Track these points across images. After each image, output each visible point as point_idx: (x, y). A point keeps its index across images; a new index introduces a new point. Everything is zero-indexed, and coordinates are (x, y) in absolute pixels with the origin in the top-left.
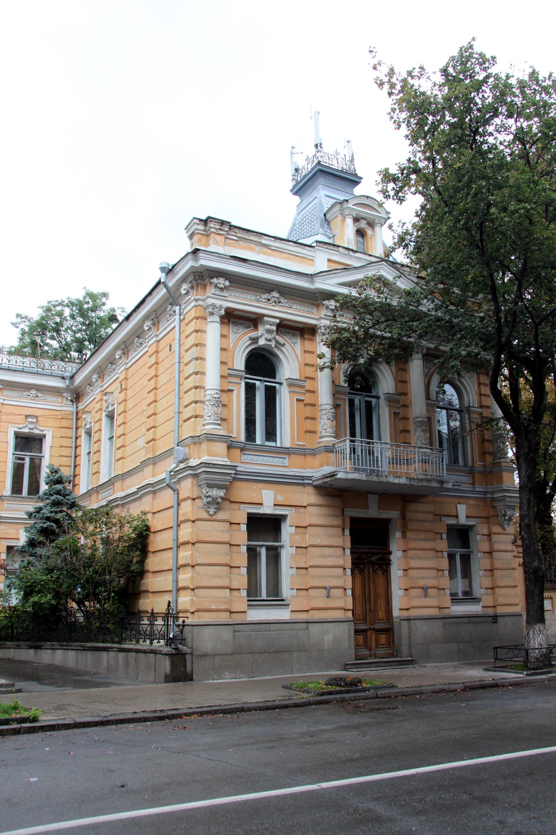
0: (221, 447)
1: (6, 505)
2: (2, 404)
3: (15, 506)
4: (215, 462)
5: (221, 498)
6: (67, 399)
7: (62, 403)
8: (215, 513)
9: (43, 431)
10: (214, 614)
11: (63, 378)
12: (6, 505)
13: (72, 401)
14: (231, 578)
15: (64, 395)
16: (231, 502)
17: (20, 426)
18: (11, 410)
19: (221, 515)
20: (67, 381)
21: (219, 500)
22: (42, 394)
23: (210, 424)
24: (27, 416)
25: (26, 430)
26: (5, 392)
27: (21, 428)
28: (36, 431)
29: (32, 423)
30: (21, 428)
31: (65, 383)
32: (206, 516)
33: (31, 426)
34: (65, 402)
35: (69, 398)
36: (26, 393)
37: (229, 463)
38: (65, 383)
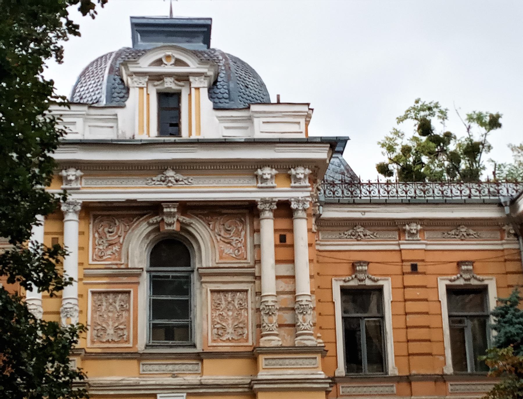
1: (450, 387)
2: (425, 250)
3: (462, 387)
6: (509, 233)
7: (502, 239)
9: (483, 280)
11: (500, 205)
12: (450, 387)
13: (516, 235)
15: (504, 228)
17: (453, 277)
20: (507, 210)
22: (474, 230)
24: (459, 264)
25: (461, 282)
26: (426, 235)
27: (454, 280)
28: (474, 282)
29: (467, 271)
30: (454, 280)
31: (503, 211)
33: (467, 276)
34: (506, 238)
35: (512, 232)
36: (453, 232)
38: (503, 211)
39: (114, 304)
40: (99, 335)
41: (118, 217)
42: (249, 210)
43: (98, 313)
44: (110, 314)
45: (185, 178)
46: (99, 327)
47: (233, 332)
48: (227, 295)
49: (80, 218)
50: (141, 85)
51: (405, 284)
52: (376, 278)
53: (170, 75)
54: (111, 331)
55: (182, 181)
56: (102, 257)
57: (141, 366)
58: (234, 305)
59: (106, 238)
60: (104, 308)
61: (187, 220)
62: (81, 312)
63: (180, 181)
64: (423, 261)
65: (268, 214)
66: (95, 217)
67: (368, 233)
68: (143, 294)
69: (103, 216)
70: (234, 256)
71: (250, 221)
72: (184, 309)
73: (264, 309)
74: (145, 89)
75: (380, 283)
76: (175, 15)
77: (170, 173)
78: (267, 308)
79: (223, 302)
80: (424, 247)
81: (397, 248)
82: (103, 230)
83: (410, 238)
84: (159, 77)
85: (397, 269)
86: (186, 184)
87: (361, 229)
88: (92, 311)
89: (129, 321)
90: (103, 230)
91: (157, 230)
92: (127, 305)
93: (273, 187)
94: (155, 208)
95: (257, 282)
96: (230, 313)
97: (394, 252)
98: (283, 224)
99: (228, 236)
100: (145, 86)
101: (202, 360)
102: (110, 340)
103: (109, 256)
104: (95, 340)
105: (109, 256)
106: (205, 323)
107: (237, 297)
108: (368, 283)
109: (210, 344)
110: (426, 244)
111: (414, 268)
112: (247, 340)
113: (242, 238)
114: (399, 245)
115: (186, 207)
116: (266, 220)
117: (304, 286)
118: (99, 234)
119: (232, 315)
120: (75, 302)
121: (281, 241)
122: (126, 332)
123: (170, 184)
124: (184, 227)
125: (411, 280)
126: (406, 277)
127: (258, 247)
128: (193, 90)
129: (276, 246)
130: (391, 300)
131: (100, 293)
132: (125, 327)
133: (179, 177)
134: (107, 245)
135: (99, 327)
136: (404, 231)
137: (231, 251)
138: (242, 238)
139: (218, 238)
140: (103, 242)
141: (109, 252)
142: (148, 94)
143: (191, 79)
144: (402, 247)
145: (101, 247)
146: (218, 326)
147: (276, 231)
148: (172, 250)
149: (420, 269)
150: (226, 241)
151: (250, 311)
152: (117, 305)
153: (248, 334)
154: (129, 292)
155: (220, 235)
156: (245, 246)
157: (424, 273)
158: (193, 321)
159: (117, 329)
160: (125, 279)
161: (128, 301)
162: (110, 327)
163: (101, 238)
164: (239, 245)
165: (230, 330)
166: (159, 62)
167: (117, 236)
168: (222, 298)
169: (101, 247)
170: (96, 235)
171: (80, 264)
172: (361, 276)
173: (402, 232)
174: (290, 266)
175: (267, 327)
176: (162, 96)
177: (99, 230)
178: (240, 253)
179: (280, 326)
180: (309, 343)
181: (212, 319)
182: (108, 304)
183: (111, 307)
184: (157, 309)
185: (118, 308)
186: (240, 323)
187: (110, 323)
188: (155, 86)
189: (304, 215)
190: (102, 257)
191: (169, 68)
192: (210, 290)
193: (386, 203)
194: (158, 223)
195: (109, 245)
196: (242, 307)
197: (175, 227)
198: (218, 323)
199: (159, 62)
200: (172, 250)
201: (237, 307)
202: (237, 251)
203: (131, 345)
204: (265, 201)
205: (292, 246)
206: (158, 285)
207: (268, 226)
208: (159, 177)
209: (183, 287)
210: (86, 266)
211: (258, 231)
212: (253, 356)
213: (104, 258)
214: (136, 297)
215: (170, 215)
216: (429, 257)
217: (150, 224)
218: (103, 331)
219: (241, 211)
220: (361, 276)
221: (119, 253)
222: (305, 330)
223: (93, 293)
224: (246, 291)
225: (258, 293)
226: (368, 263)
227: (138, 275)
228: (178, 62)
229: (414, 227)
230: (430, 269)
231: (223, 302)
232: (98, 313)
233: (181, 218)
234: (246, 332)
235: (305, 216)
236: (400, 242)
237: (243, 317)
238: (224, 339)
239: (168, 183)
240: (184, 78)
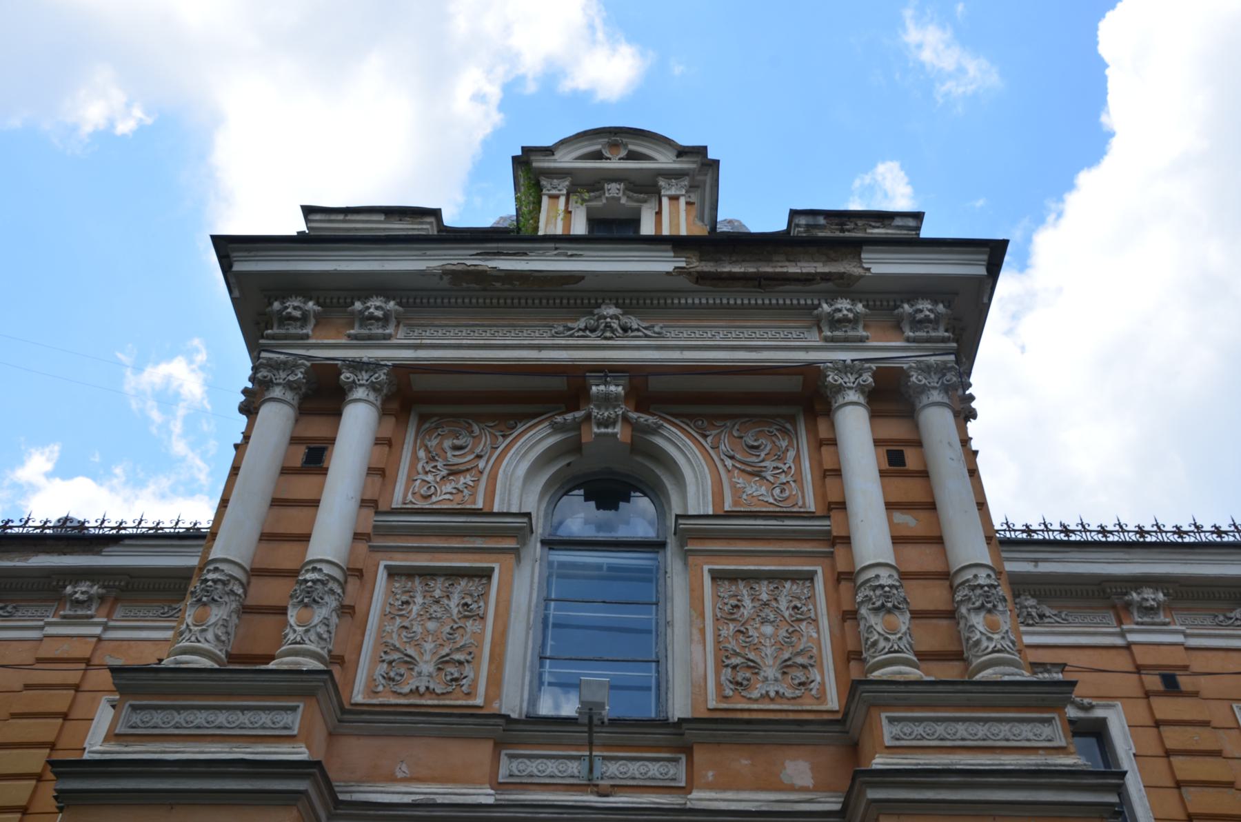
2: (1188, 649)
18: (1215, 663)
39: (445, 601)
40: (392, 674)
41: (479, 418)
43: (398, 620)
44: (431, 625)
45: (645, 324)
46: (396, 656)
47: (779, 676)
48: (756, 587)
49: (384, 412)
50: (554, 192)
51: (1159, 716)
52: (1086, 701)
54: (427, 667)
55: (638, 330)
56: (430, 496)
57: (504, 760)
58: (777, 610)
59: (446, 459)
60: (415, 609)
62: (346, 610)
63: (633, 331)
64: (1185, 668)
65: (852, 396)
66: (423, 419)
69: (442, 416)
70: (771, 500)
71: (808, 431)
73: (868, 599)
74: (562, 200)
75: (1099, 713)
78: (878, 592)
79: (747, 602)
80: (1179, 639)
81: (1118, 641)
82: (440, 443)
83: (1146, 619)
86: (646, 336)
88: (384, 615)
89: (480, 646)
90: (440, 443)
91: (574, 447)
92: (482, 604)
93: (862, 339)
95: (840, 551)
96: (768, 629)
97: (1113, 652)
98: (895, 430)
99: (754, 459)
100: (565, 192)
101: (688, 750)
102: (422, 689)
103: (447, 496)
104: (380, 688)
105: (447, 496)
106: (697, 649)
107: (785, 592)
109: (712, 704)
110: (1186, 635)
112: (821, 697)
113: (790, 462)
114: (1122, 634)
116: (849, 409)
118: (427, 450)
119: (775, 635)
120: (337, 573)
121: (891, 464)
122: (468, 670)
123: (608, 334)
124: (642, 447)
125: (1167, 708)
126: (1155, 701)
127: (833, 473)
128: (665, 201)
129: (883, 474)
130: (1134, 751)
131: (411, 573)
132: (469, 658)
133: (634, 322)
134: (445, 472)
135: (396, 656)
136: (1128, 606)
137: (763, 490)
138: (790, 462)
139: (729, 462)
140: (435, 467)
141: (448, 487)
143: (662, 182)
144: (1132, 638)
145: (430, 478)
146: (735, 661)
147: (877, 443)
149: (1184, 682)
150: (749, 469)
151: (824, 623)
152: (454, 604)
153: (822, 684)
154: (486, 574)
155: (732, 458)
156: (798, 480)
157: (1195, 694)
158: (662, 661)
159: (443, 662)
160: (479, 543)
161: (484, 596)
162: (427, 657)
163: (433, 459)
164: (783, 478)
165: (771, 672)
167: (472, 456)
168: (745, 592)
169: (430, 478)
170: (422, 454)
173: (1121, 611)
174: (923, 515)
175: (882, 644)
177: (429, 444)
178: (787, 493)
181: (718, 642)
182: (429, 600)
183: (435, 607)
185: (455, 611)
186: (798, 654)
187: (429, 646)
188: (584, 200)
190: (430, 496)
191: (614, 164)
192: (710, 571)
194: (577, 426)
195: (449, 475)
196: (799, 615)
198: (736, 654)
199: (598, 156)
201: (786, 614)
202: (777, 491)
203: (479, 701)
204: (844, 368)
205: (924, 474)
207: (855, 427)
208: (582, 323)
210: (382, 507)
211: (833, 442)
212: (843, 734)
213: (434, 499)
215: (607, 400)
216: (1198, 663)
217: (557, 428)
218: (406, 666)
219: (783, 410)
221: (473, 489)
222: (999, 651)
223: (393, 573)
224: (809, 577)
225: (846, 577)
230: (1205, 685)
231: (747, 602)
232: (398, 620)
233: (633, 415)
234: (818, 678)
236: (1125, 627)
237: (804, 639)
238: (755, 694)
239: (604, 331)
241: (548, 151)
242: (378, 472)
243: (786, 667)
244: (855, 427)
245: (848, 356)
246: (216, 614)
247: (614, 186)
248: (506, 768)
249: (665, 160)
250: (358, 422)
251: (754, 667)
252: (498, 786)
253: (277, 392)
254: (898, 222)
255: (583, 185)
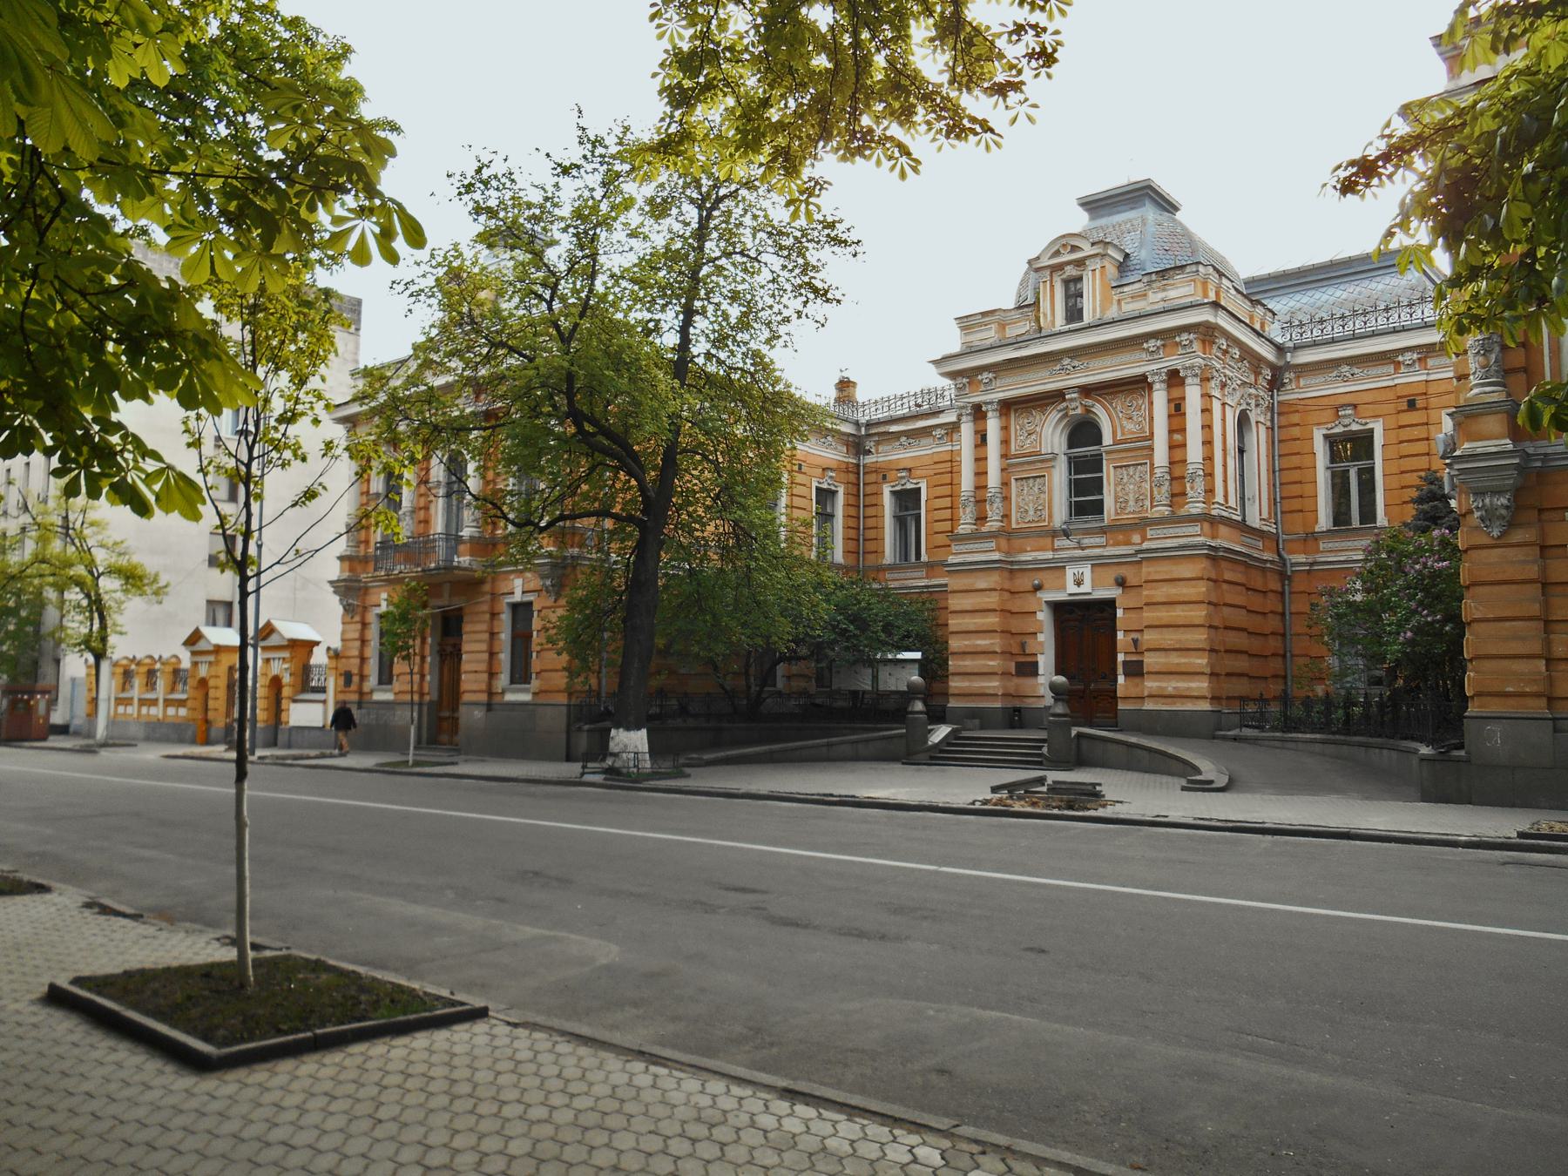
0: (1494, 424)
4: (1479, 451)
5: (1507, 507)
8: (1503, 534)
10: (1512, 701)
14: (1548, 643)
16: (1541, 511)
19: (1518, 536)
21: (1503, 512)
23: (1477, 385)
26: (1430, 362)
32: (1485, 540)
37: (1510, 447)
42: (1140, 384)
53: (1069, 263)
54: (1031, 512)
61: (1089, 402)
67: (1356, 371)
68: (1059, 477)
72: (1097, 486)
76: (1133, 180)
77: (1066, 361)
80: (1424, 378)
81: (1391, 383)
84: (1059, 267)
85: (1390, 408)
87: (1347, 368)
91: (1066, 415)
94: (1058, 396)
108: (1355, 427)
111: (1412, 405)
115: (1086, 391)
117: (1194, 453)
127: (1152, 419)
129: (1170, 416)
133: (1076, 363)
142: (1052, 286)
147: (1169, 401)
148: (1083, 432)
149: (1420, 403)
159: (1036, 510)
160: (1039, 465)
165: (1131, 503)
166: (1057, 253)
171: (1005, 456)
172: (1346, 421)
176: (1067, 282)
179: (1173, 495)
180: (1194, 511)
184: (1077, 487)
189: (1197, 380)
193: (1374, 334)
197: (1079, 411)
199: (1057, 253)
200: (1083, 432)
206: (1076, 465)
207: (1160, 397)
209: (1096, 464)
214: (1050, 481)
215: (1072, 400)
220: (1346, 421)
226: (1355, 406)
227: (1054, 459)
228: (1075, 248)
229: (1408, 357)
230: (1434, 402)
235: (1197, 380)
240: (1080, 263)
241: (1038, 258)
242: (1005, 442)
243: (1137, 501)
244: (1160, 397)
245: (1155, 367)
246: (968, 510)
247: (1068, 268)
248: (1057, 543)
249: (1088, 250)
250: (993, 425)
251: (1126, 502)
252: (1054, 550)
253: (964, 419)
254: (1188, 269)
255: (1056, 269)
